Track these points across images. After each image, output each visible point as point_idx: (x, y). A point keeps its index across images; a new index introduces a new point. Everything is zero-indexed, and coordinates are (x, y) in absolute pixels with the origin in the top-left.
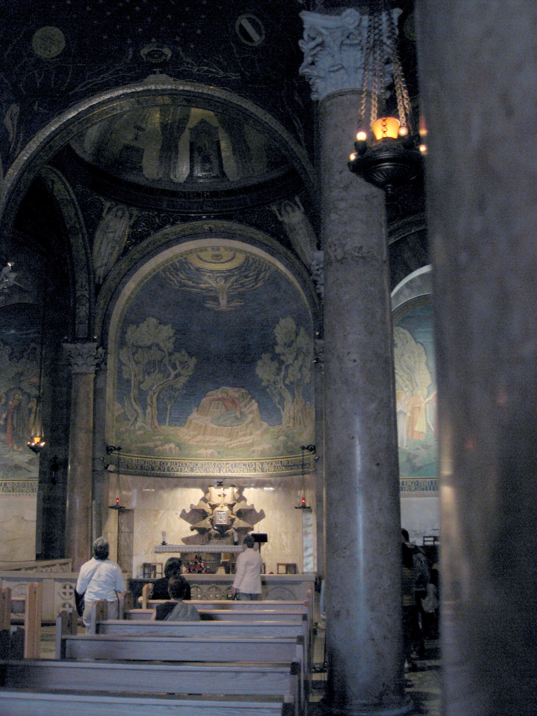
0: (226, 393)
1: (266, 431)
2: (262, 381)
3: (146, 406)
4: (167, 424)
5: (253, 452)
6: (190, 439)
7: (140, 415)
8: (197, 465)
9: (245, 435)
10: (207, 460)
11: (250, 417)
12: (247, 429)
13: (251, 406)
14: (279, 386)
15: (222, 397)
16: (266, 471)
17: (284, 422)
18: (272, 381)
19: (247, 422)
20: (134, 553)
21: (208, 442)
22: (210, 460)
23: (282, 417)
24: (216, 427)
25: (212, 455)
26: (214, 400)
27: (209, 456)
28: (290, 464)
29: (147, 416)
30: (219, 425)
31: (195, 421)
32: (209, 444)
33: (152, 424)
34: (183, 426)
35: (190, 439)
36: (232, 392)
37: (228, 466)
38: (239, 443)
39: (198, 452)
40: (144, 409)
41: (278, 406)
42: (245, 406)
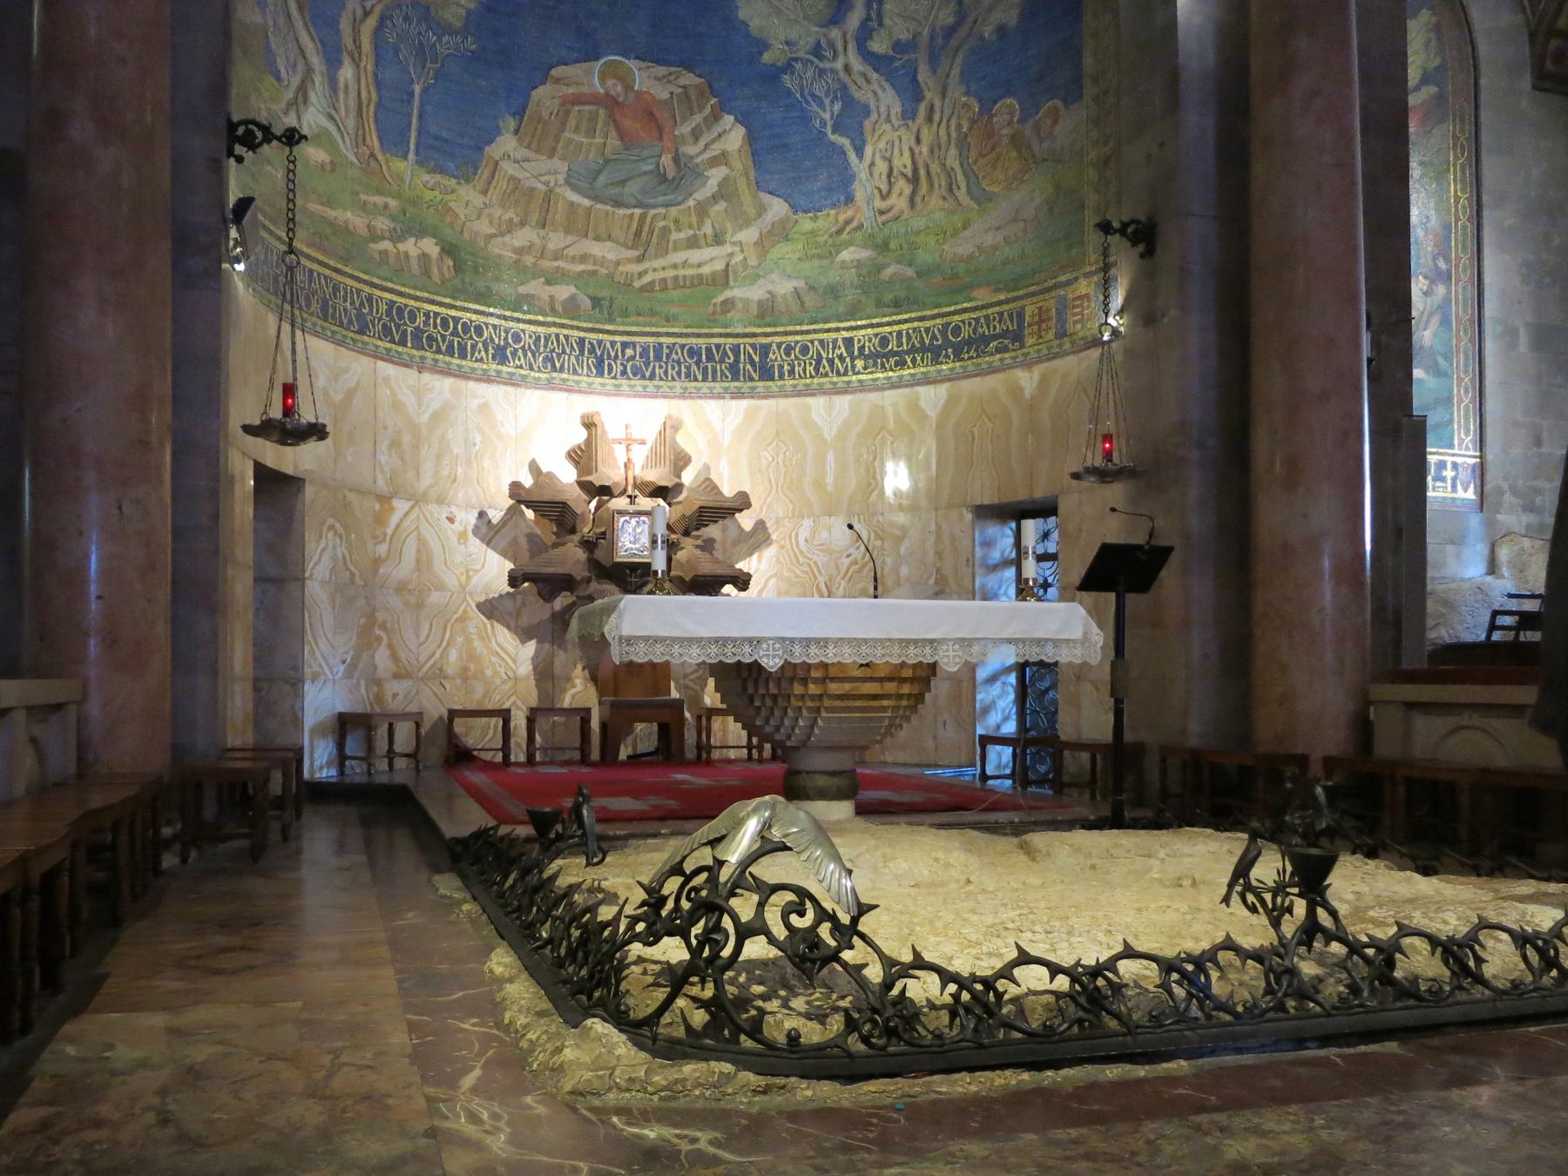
0: (621, 79)
1: (780, 232)
2: (763, 46)
3: (338, 50)
4: (411, 156)
5: (728, 304)
6: (495, 236)
7: (318, 78)
8: (517, 338)
9: (693, 243)
10: (555, 324)
11: (716, 175)
12: (700, 224)
13: (720, 136)
14: (839, 65)
15: (607, 94)
16: (781, 377)
17: (860, 195)
18: (806, 43)
19: (703, 193)
20: (307, 670)
21: (556, 256)
22: (563, 326)
23: (853, 177)
24: (586, 202)
25: (570, 308)
26: (577, 100)
27: (559, 308)
28: (892, 345)
29: (341, 95)
30: (595, 198)
31: (508, 168)
32: (561, 263)
33: (360, 139)
34: (468, 181)
35: (495, 236)
36: (646, 79)
37: (629, 352)
38: (670, 273)
39: (522, 290)
40: (333, 63)
41: (832, 137)
42: (696, 135)
